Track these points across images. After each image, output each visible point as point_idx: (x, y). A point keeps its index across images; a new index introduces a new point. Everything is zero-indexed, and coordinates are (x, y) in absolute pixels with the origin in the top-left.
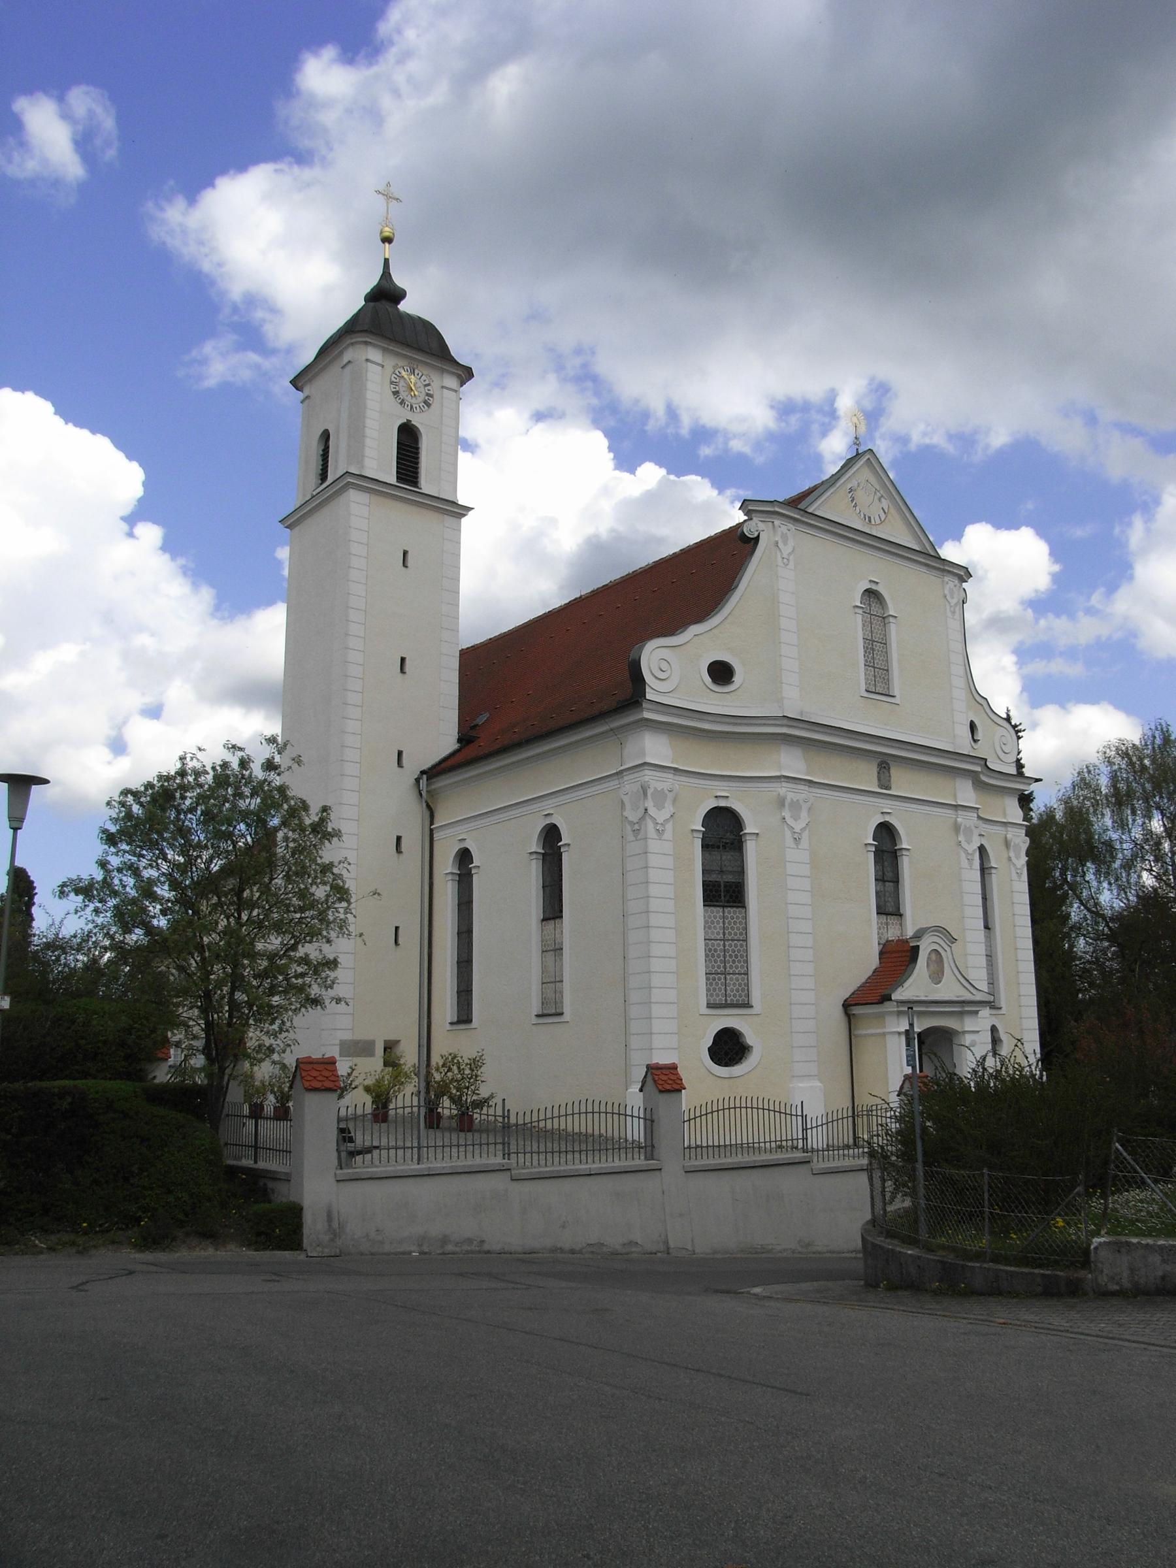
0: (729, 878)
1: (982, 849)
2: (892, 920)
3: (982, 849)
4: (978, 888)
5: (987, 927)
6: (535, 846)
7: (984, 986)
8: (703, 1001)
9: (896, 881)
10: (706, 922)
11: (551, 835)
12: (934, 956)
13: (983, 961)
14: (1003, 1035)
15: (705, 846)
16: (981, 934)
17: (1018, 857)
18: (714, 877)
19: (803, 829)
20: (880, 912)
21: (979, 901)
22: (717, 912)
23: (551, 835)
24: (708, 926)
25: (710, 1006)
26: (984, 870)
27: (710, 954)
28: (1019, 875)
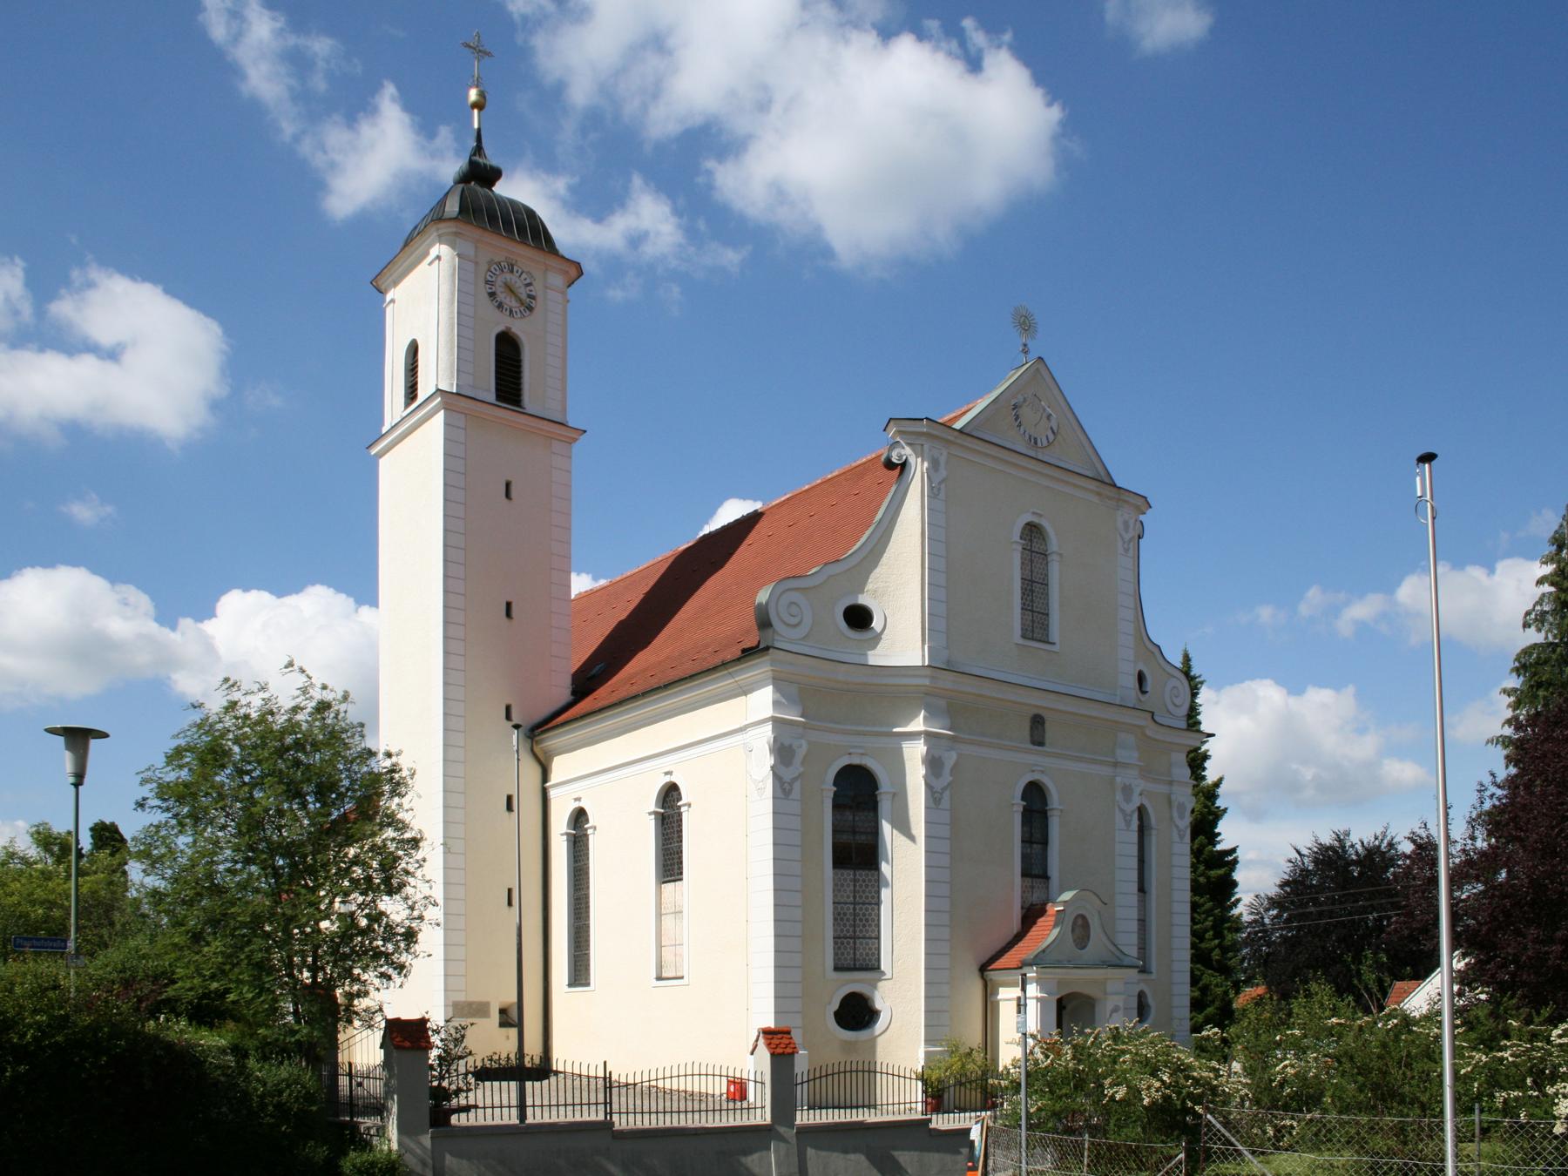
0: (862, 839)
1: (1141, 811)
2: (1038, 882)
3: (1141, 811)
4: (1134, 850)
5: (1142, 889)
6: (651, 804)
7: (1133, 952)
8: (830, 963)
9: (1045, 842)
10: (835, 885)
11: (670, 794)
12: (1080, 922)
13: (1134, 926)
14: (1151, 1001)
15: (837, 806)
16: (1133, 899)
17: (1182, 817)
18: (845, 838)
19: (944, 789)
20: (1024, 874)
21: (1134, 863)
22: (848, 874)
23: (670, 794)
24: (837, 888)
25: (837, 969)
26: (1142, 830)
27: (838, 918)
28: (1182, 837)
